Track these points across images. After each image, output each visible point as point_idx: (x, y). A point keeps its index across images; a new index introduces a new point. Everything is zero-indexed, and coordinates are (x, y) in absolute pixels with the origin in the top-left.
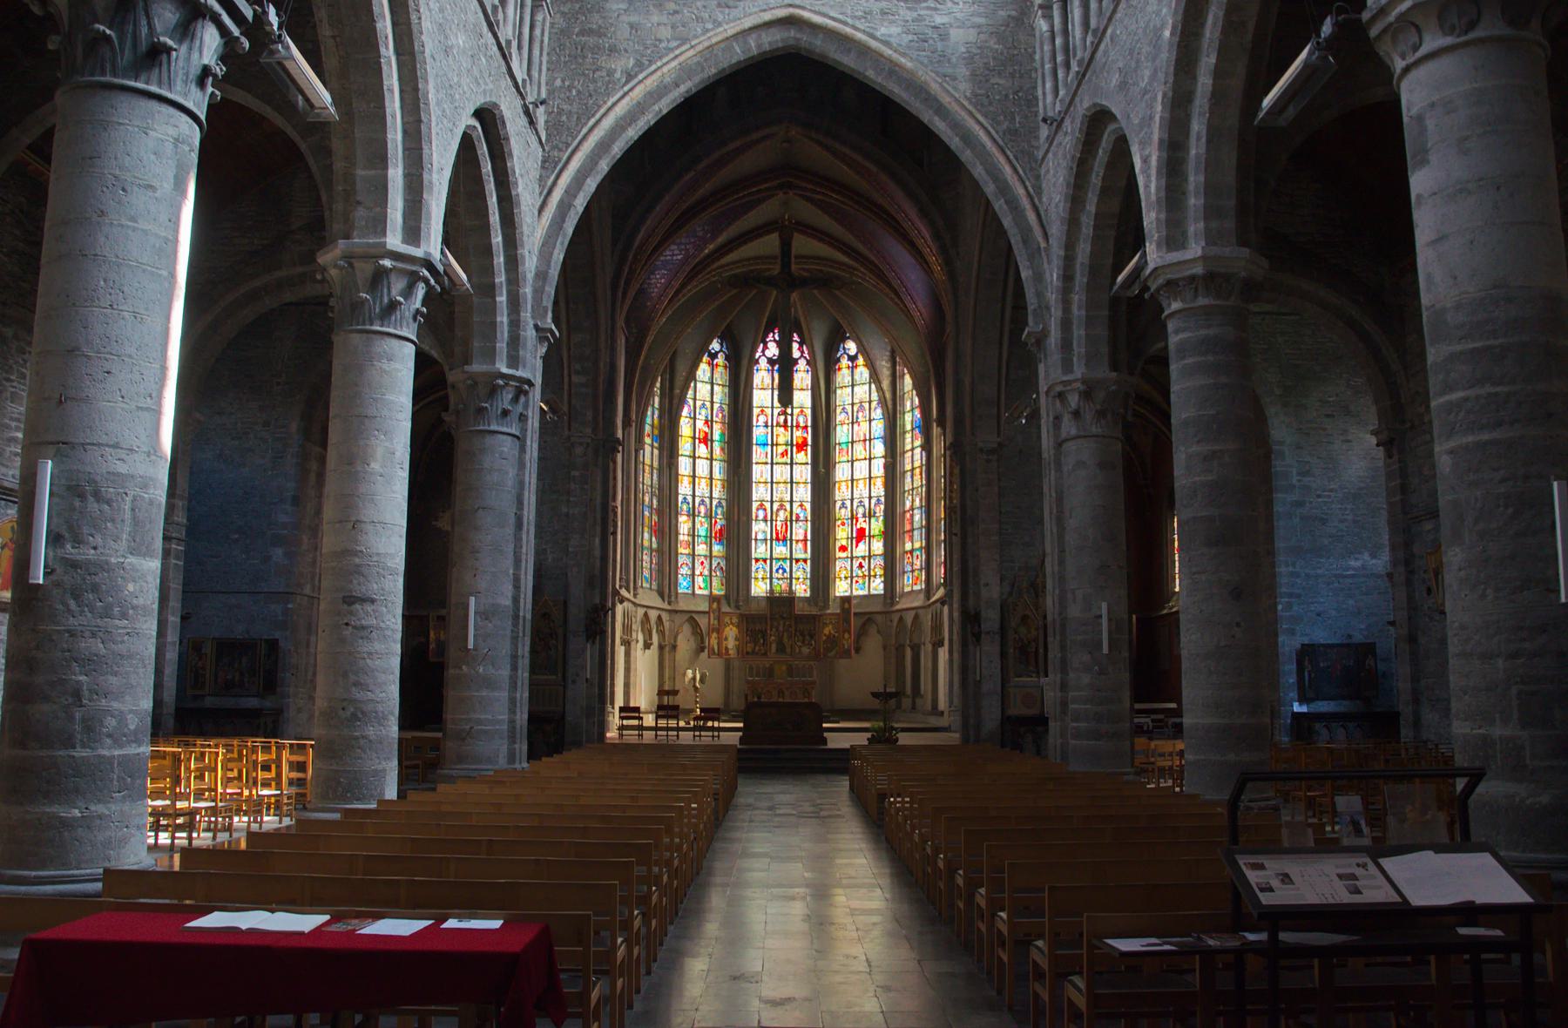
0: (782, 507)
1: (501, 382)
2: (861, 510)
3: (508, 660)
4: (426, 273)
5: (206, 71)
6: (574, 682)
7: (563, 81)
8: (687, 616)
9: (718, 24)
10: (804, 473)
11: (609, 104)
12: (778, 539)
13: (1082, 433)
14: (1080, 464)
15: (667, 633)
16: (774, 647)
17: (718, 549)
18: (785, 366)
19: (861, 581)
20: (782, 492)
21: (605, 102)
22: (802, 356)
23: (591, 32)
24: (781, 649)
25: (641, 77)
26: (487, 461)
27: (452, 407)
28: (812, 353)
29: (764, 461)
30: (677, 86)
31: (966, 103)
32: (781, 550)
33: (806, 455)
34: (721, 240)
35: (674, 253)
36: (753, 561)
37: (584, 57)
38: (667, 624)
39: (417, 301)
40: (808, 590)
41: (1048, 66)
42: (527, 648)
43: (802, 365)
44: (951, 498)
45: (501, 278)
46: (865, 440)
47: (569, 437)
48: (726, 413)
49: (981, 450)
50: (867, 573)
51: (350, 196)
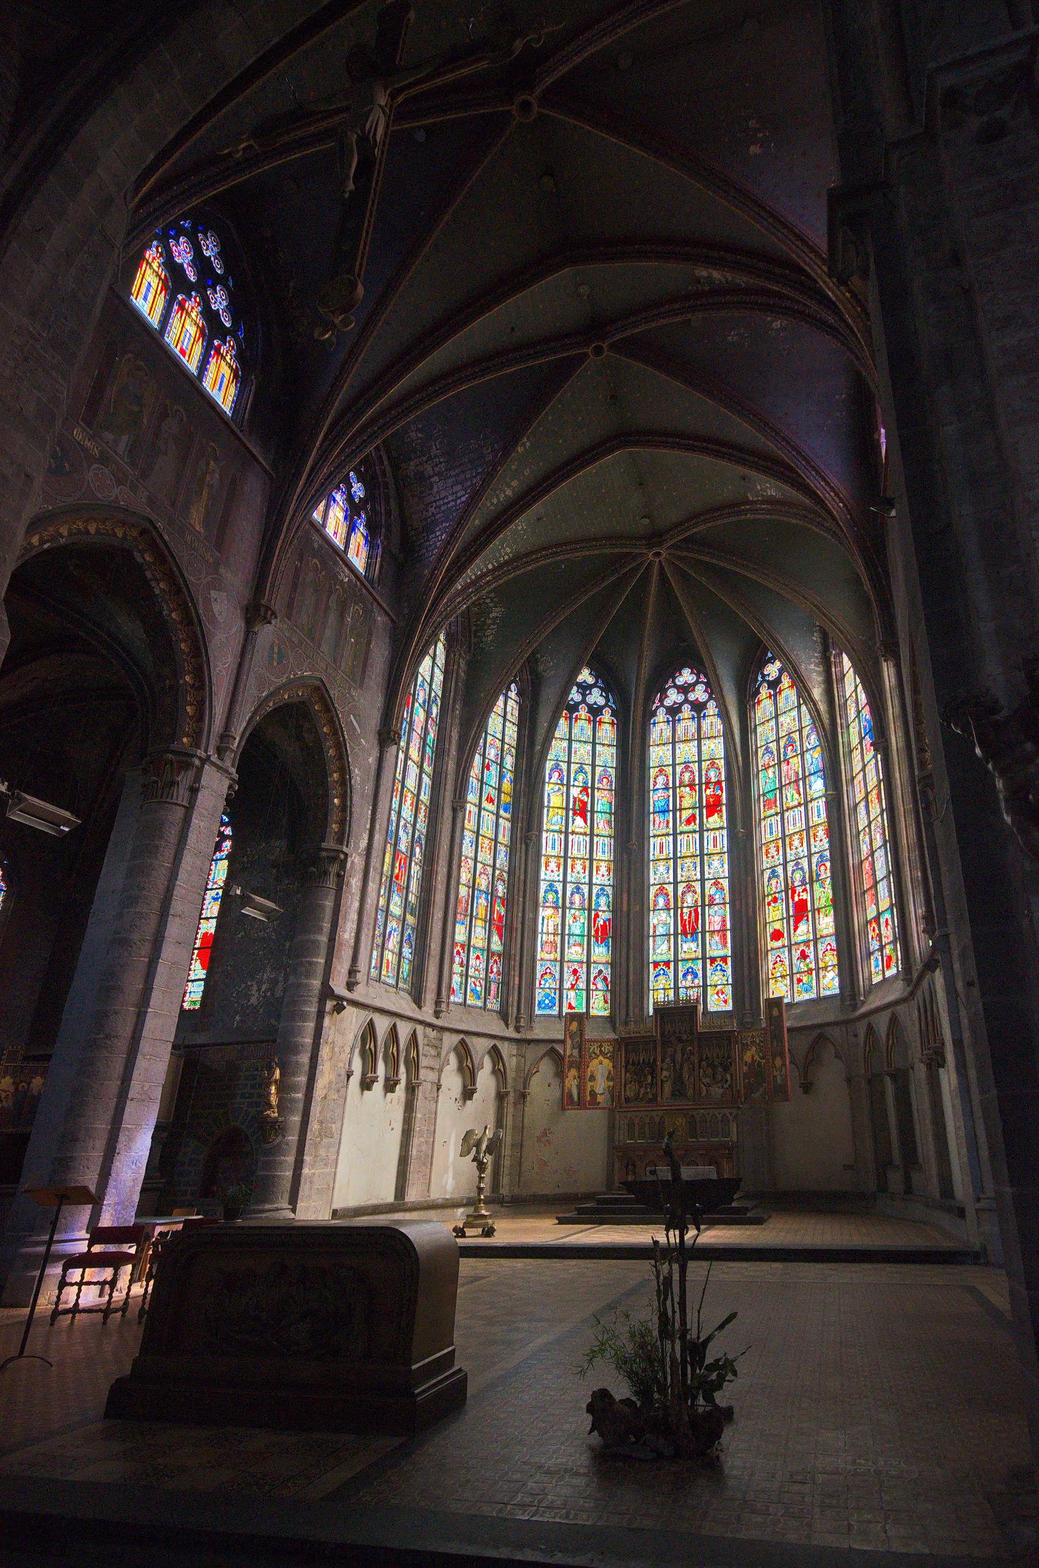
0: (689, 888)
12: (685, 933)
16: (667, 1088)
19: (805, 979)
20: (689, 870)
24: (679, 1092)
29: (664, 831)
33: (721, 817)
36: (651, 966)
40: (730, 1002)
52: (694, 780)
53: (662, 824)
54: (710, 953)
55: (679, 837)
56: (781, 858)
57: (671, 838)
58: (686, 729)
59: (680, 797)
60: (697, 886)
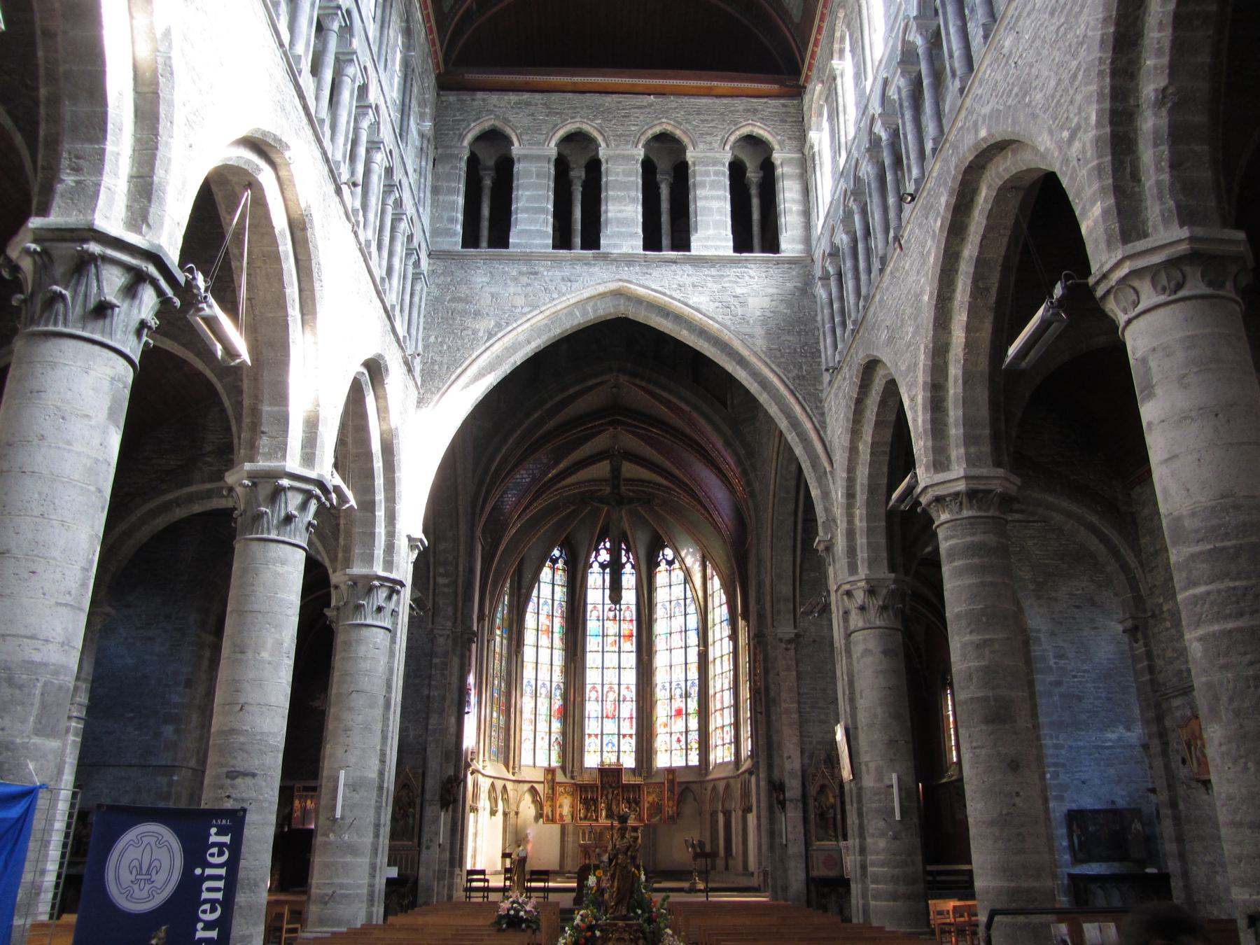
1: (377, 583)
2: (678, 692)
3: (371, 829)
4: (318, 492)
5: (143, 324)
6: (428, 848)
7: (436, 338)
8: (527, 786)
9: (561, 294)
10: (630, 660)
11: (474, 356)
12: (607, 717)
13: (868, 625)
14: (867, 652)
15: (511, 801)
16: (604, 813)
17: (557, 726)
18: (615, 568)
21: (470, 355)
22: (628, 561)
23: (460, 300)
25: (499, 335)
26: (362, 650)
27: (333, 603)
28: (636, 558)
29: (596, 649)
30: (529, 343)
31: (763, 356)
32: (610, 726)
34: (562, 466)
35: (523, 476)
37: (454, 319)
38: (511, 793)
39: (310, 515)
41: (828, 326)
42: (389, 816)
43: (628, 569)
44: (755, 681)
45: (380, 496)
47: (432, 630)
48: (564, 609)
49: (781, 640)
50: (684, 747)
51: (255, 429)
54: (622, 732)
60: (616, 687)
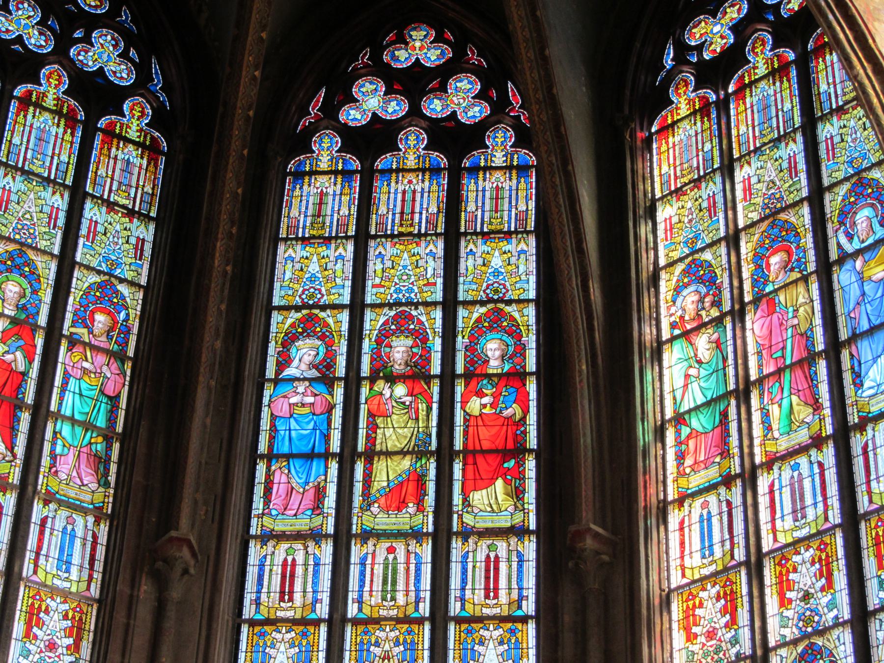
29: (303, 524)
33: (518, 494)
46: (809, 360)
52: (427, 360)
53: (295, 499)
55: (356, 551)
56: (745, 634)
57: (326, 551)
58: (409, 199)
59: (371, 415)
